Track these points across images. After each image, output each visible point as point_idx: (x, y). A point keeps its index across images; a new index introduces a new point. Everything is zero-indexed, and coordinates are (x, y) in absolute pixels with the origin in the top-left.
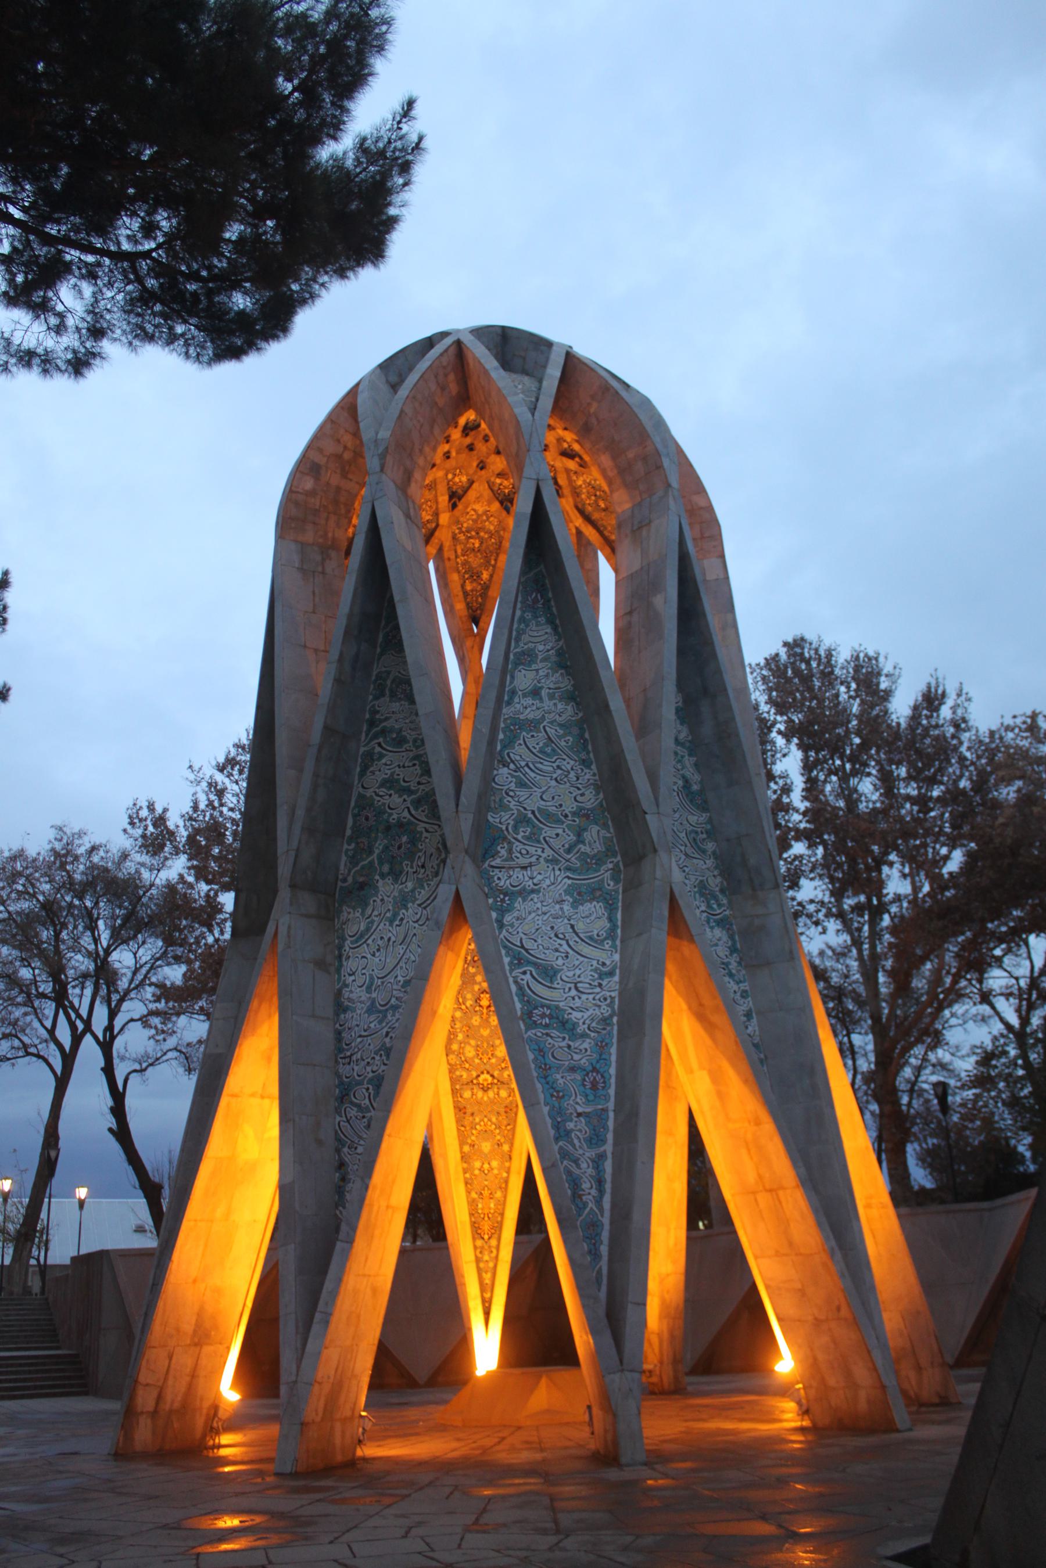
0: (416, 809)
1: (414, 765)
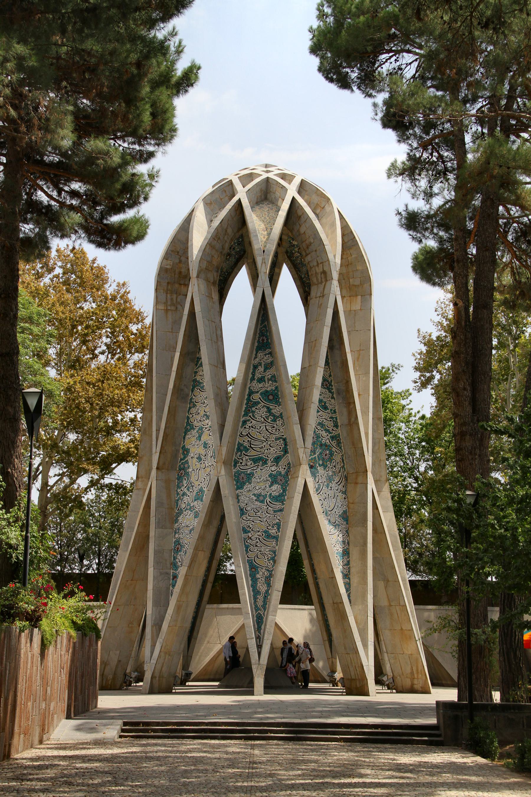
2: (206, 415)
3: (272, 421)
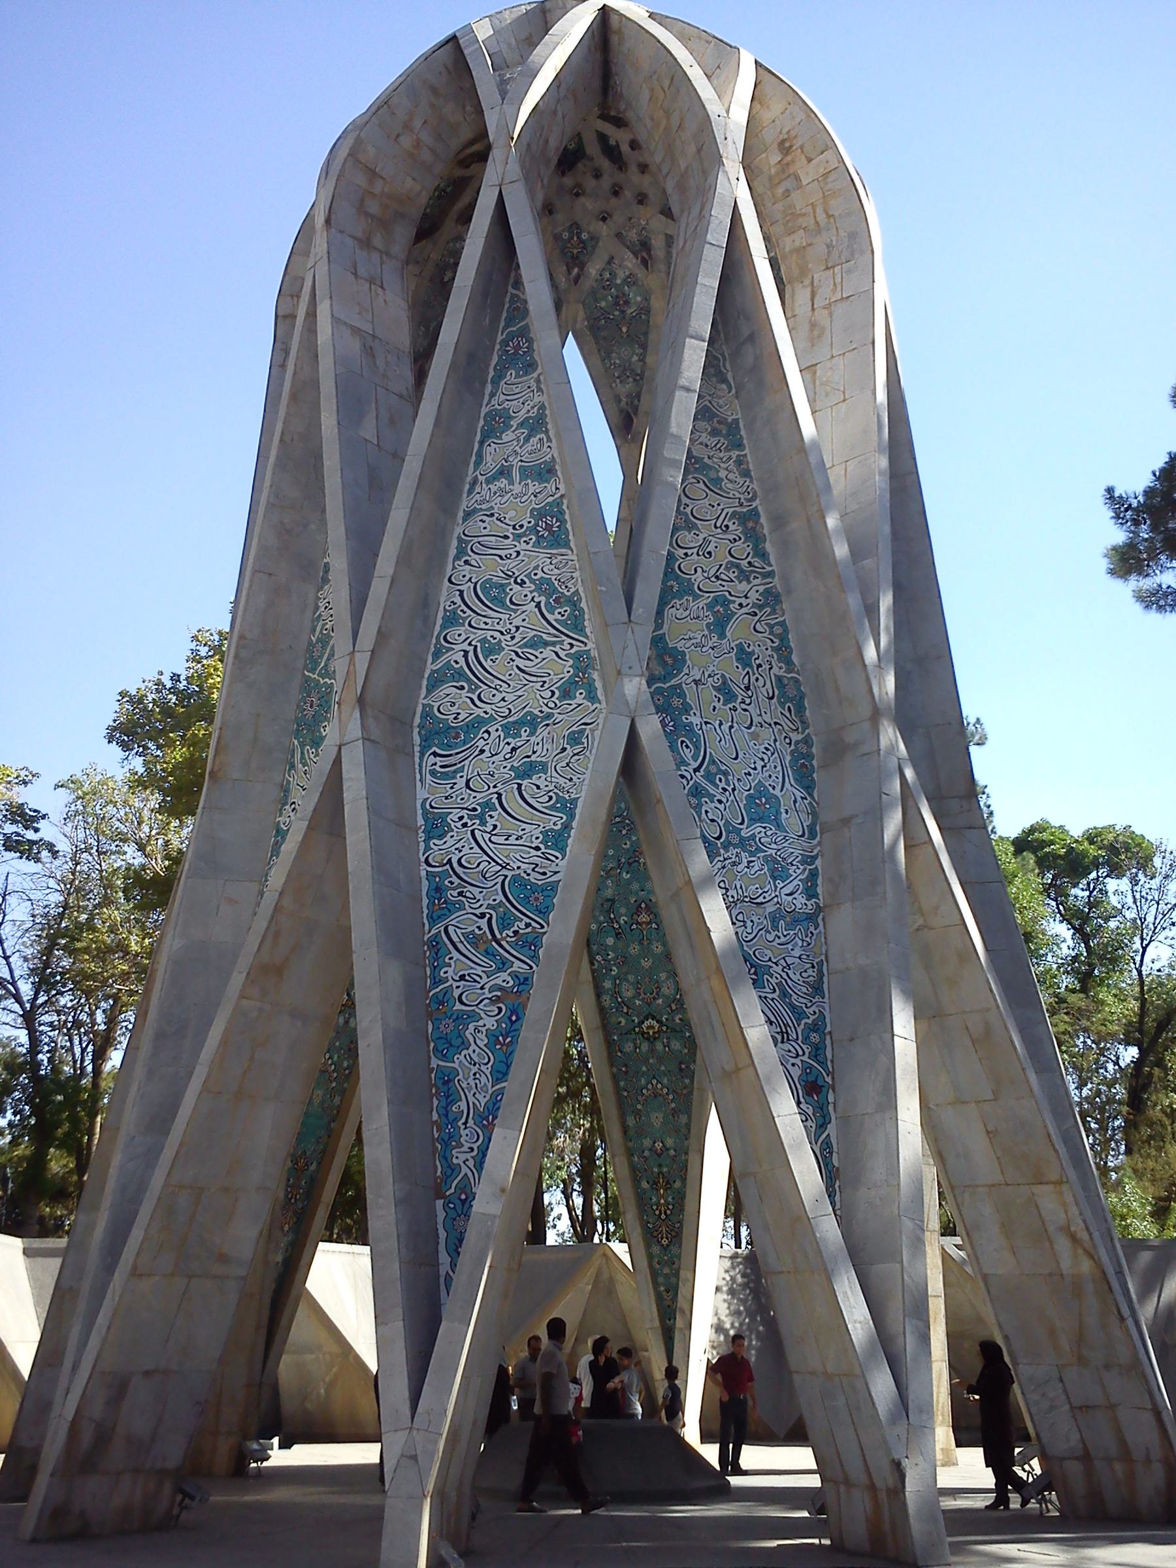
2: (738, 566)
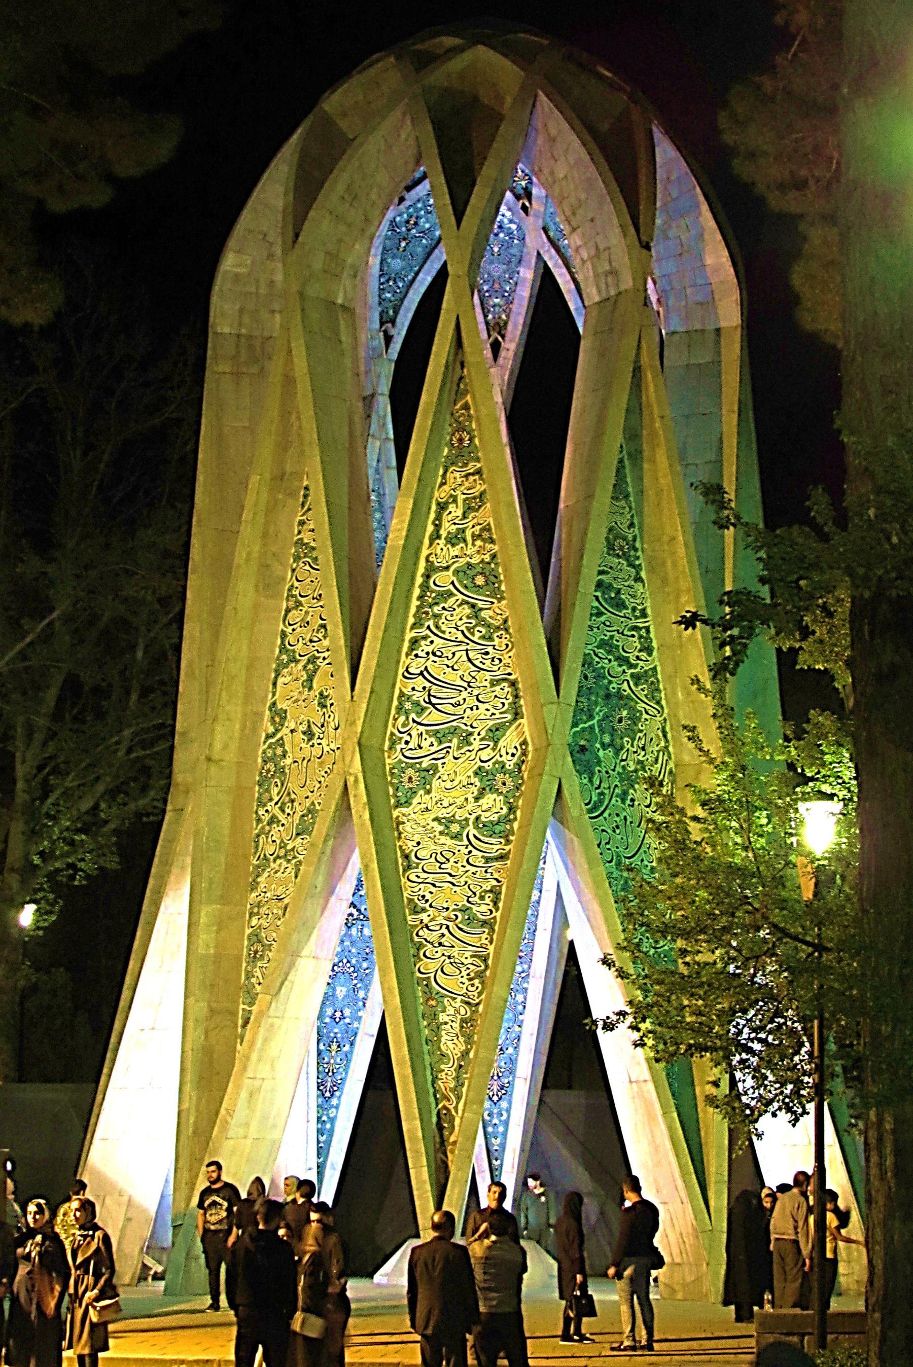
0: (636, 685)
1: (633, 636)
3: (483, 637)
